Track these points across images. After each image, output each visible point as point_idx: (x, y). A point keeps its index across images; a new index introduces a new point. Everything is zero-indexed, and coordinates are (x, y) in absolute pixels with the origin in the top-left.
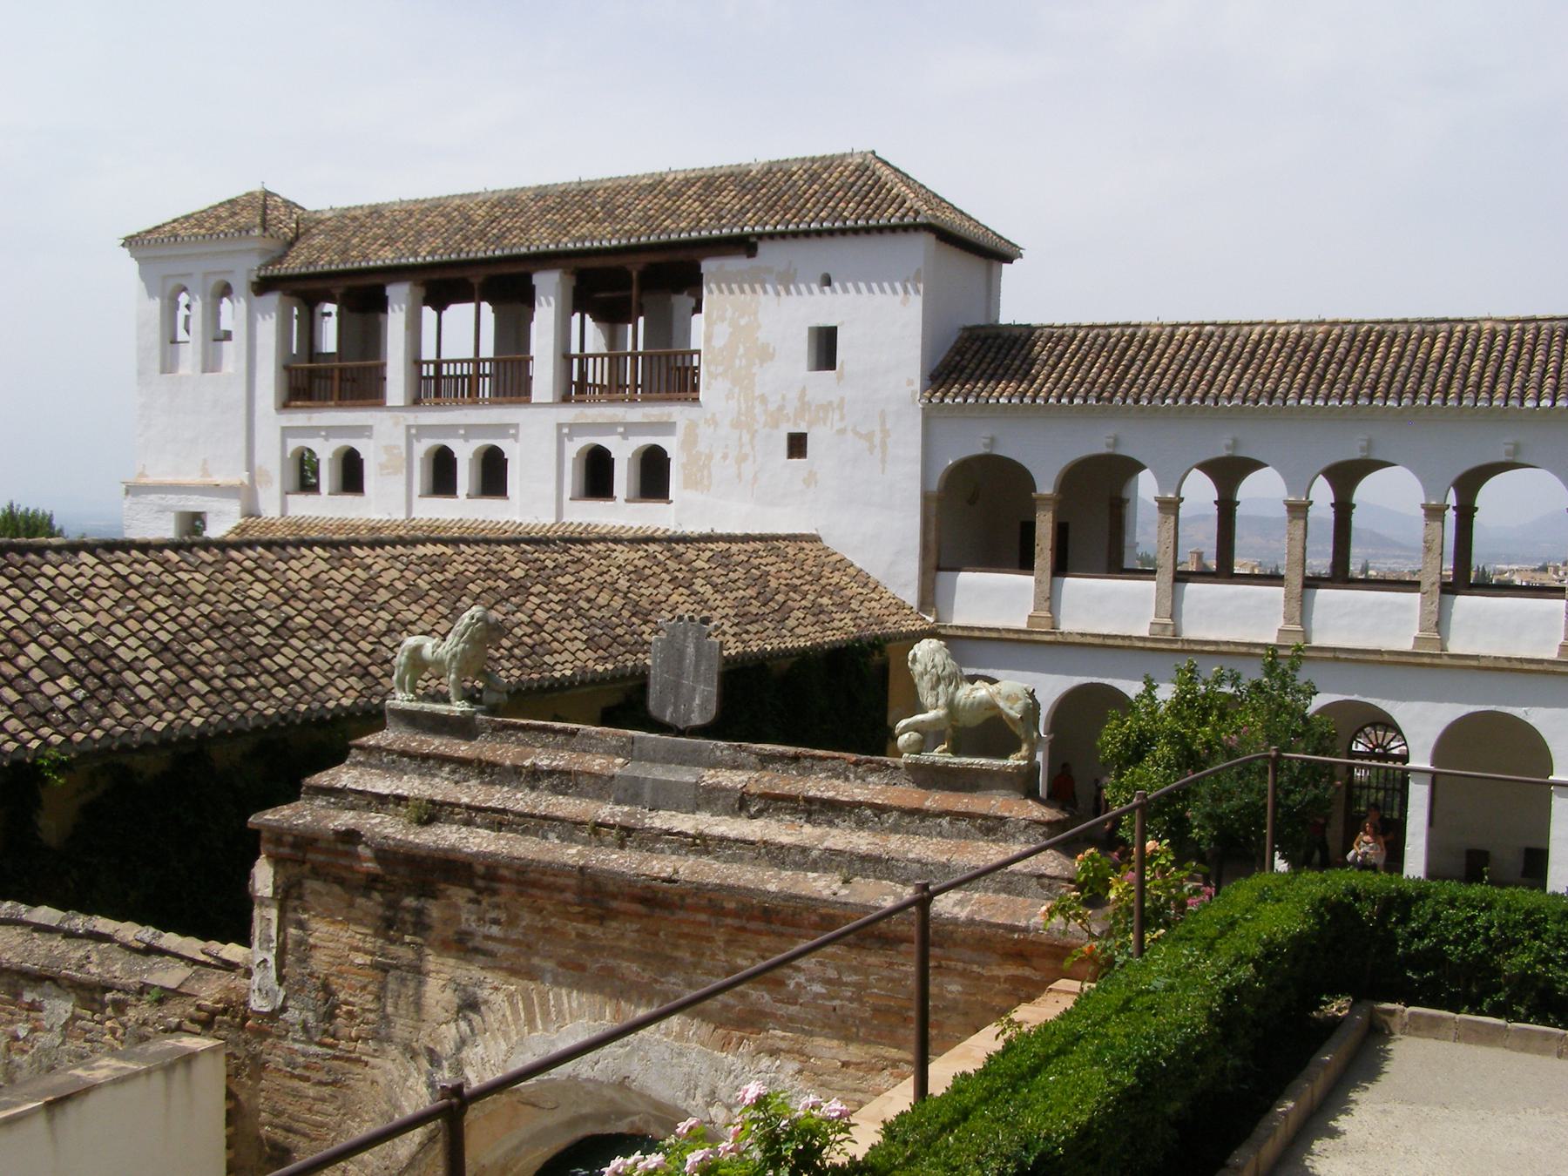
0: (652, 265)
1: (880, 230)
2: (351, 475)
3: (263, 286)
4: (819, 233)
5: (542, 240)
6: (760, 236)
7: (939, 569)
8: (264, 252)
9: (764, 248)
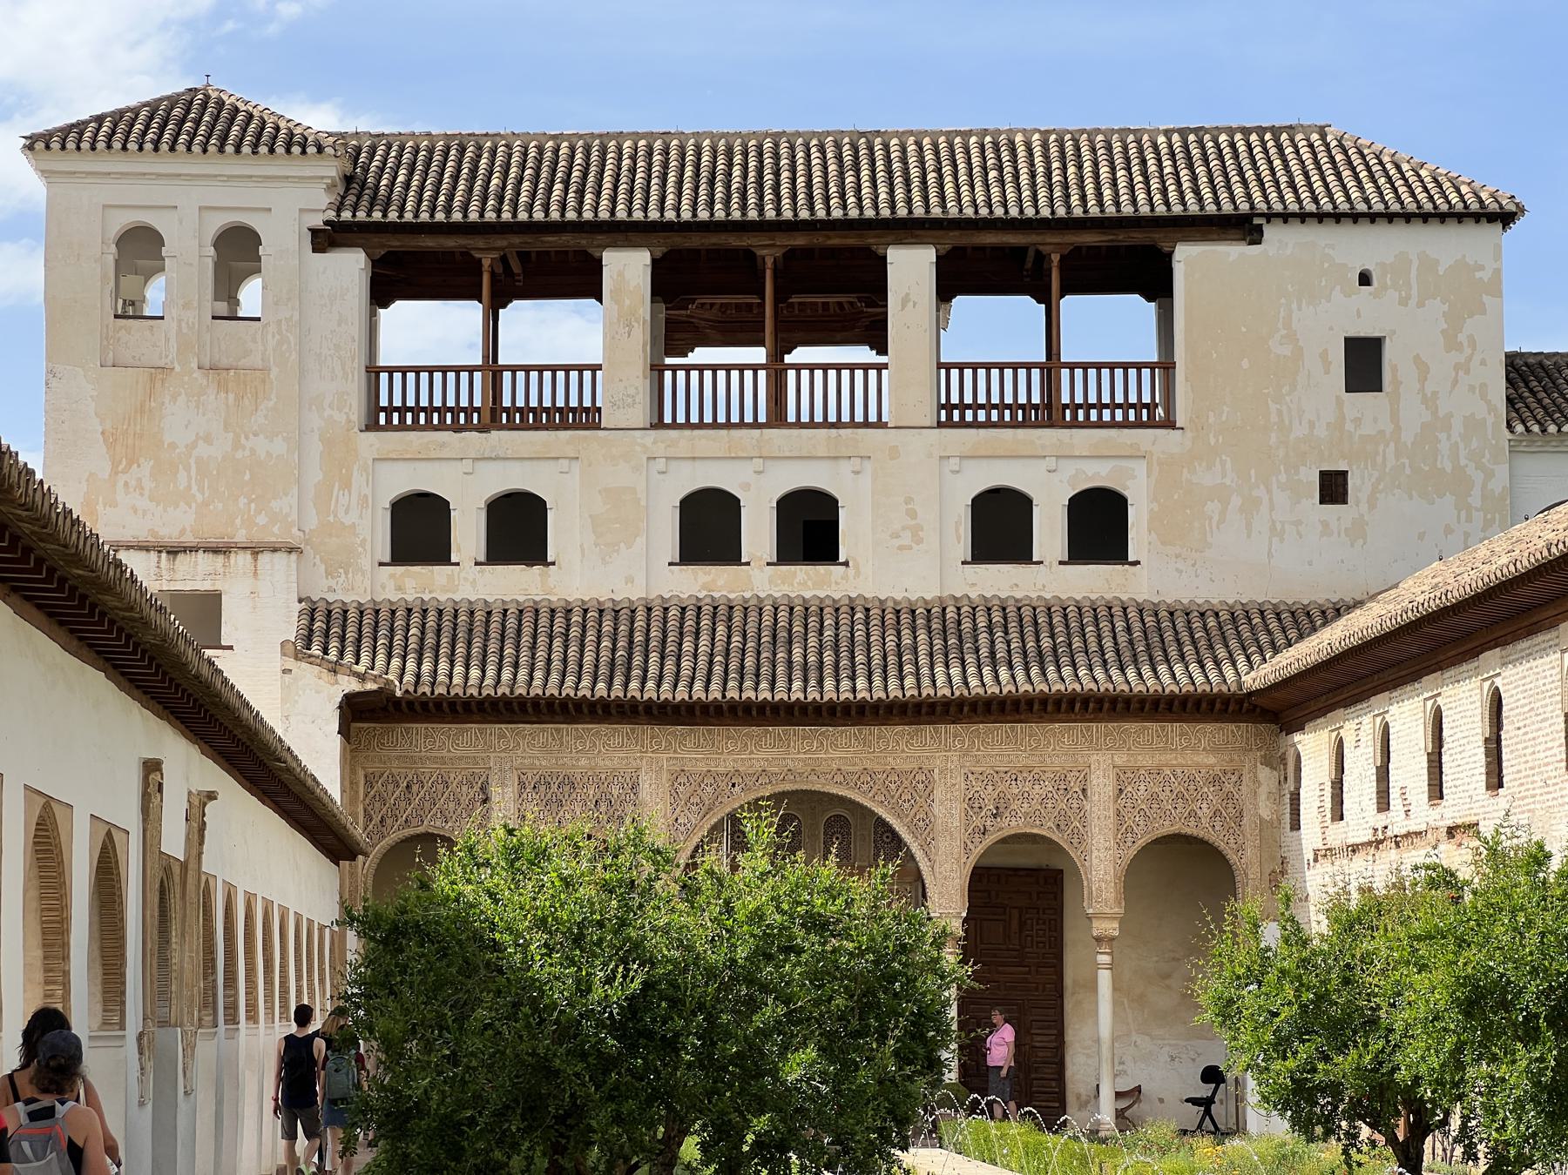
0: (1078, 249)
2: (518, 528)
3: (327, 238)
6: (1270, 216)
9: (1271, 232)
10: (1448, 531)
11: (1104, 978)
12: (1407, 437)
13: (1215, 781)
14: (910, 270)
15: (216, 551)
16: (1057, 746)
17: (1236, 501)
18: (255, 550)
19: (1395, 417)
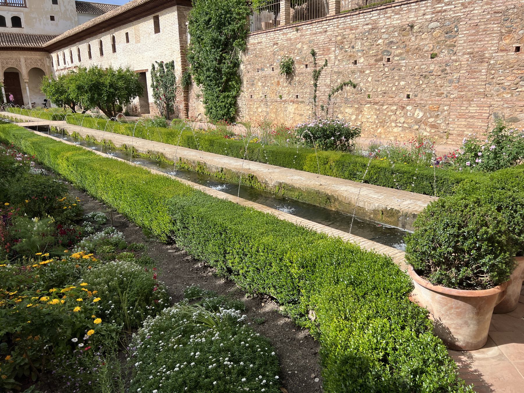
11: (27, 88)
12: (62, 12)
13: (40, 60)
16: (15, 55)
17: (38, 19)
19: (60, 9)
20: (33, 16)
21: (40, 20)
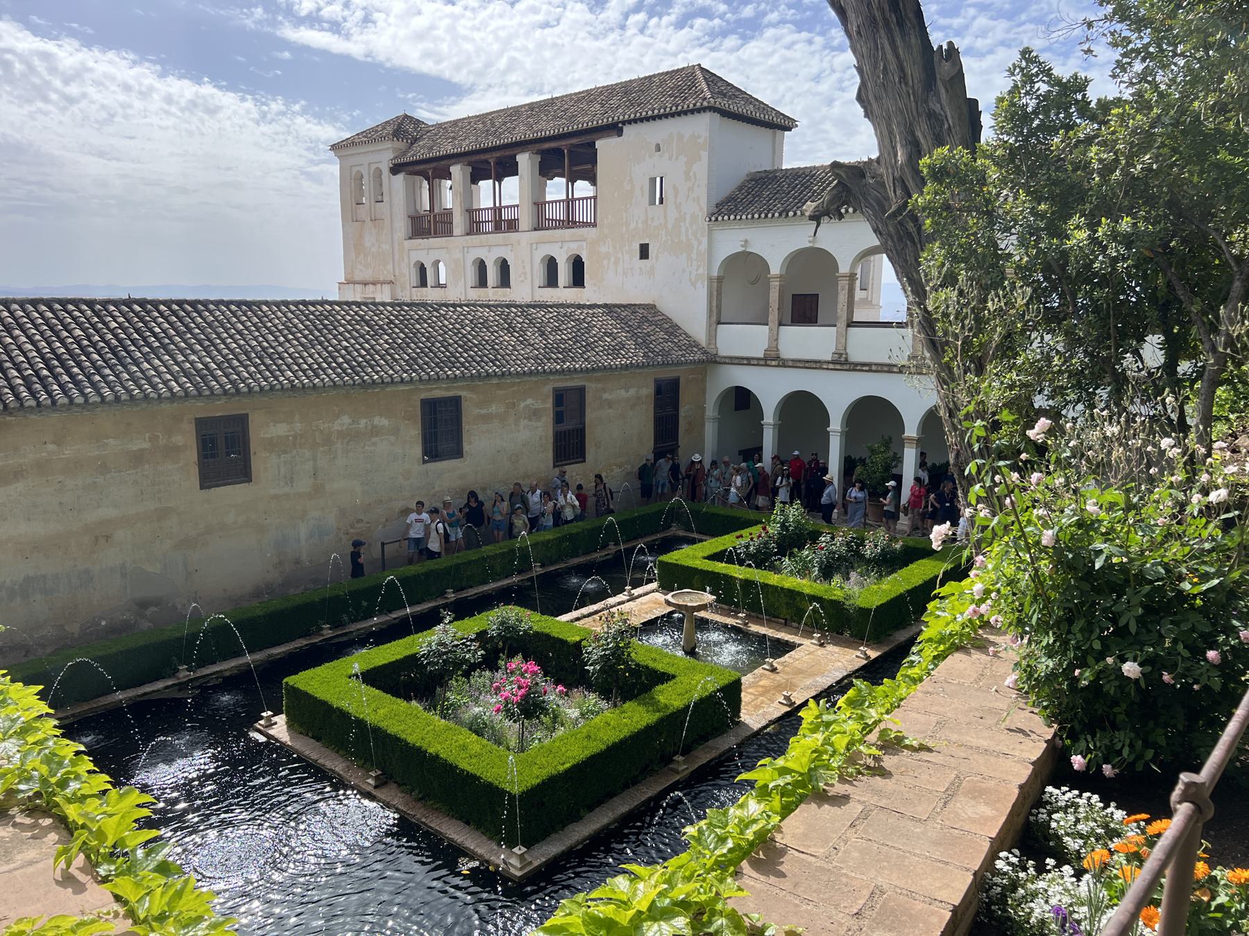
1: (685, 113)
3: (395, 170)
4: (654, 118)
5: (521, 133)
6: (624, 123)
7: (719, 323)
8: (394, 150)
9: (626, 129)
10: (684, 271)
12: (670, 226)
14: (524, 160)
15: (374, 284)
17: (613, 259)
18: (383, 283)
19: (665, 217)
20: (604, 249)
21: (616, 263)
